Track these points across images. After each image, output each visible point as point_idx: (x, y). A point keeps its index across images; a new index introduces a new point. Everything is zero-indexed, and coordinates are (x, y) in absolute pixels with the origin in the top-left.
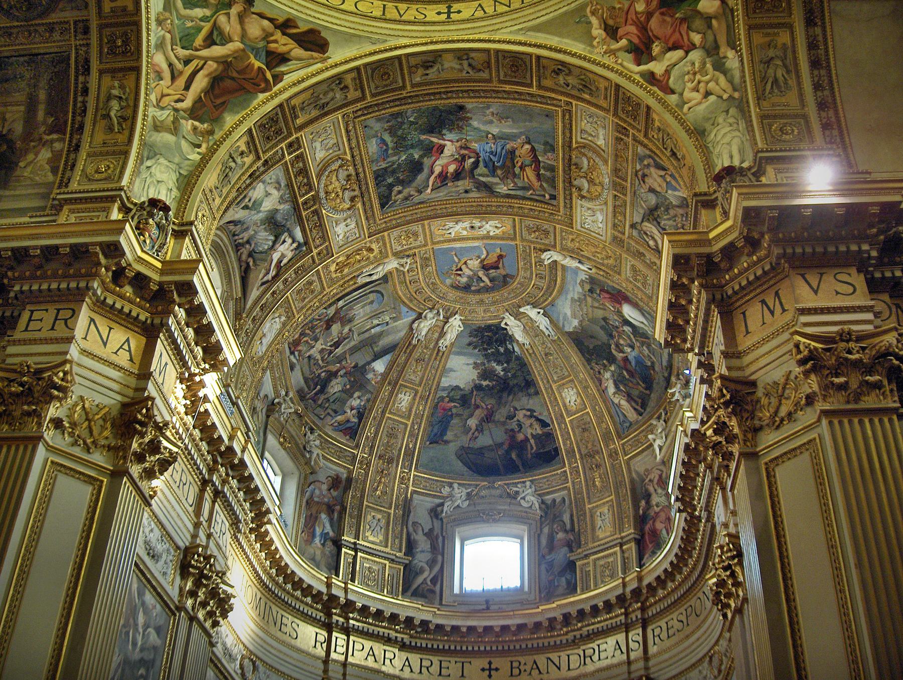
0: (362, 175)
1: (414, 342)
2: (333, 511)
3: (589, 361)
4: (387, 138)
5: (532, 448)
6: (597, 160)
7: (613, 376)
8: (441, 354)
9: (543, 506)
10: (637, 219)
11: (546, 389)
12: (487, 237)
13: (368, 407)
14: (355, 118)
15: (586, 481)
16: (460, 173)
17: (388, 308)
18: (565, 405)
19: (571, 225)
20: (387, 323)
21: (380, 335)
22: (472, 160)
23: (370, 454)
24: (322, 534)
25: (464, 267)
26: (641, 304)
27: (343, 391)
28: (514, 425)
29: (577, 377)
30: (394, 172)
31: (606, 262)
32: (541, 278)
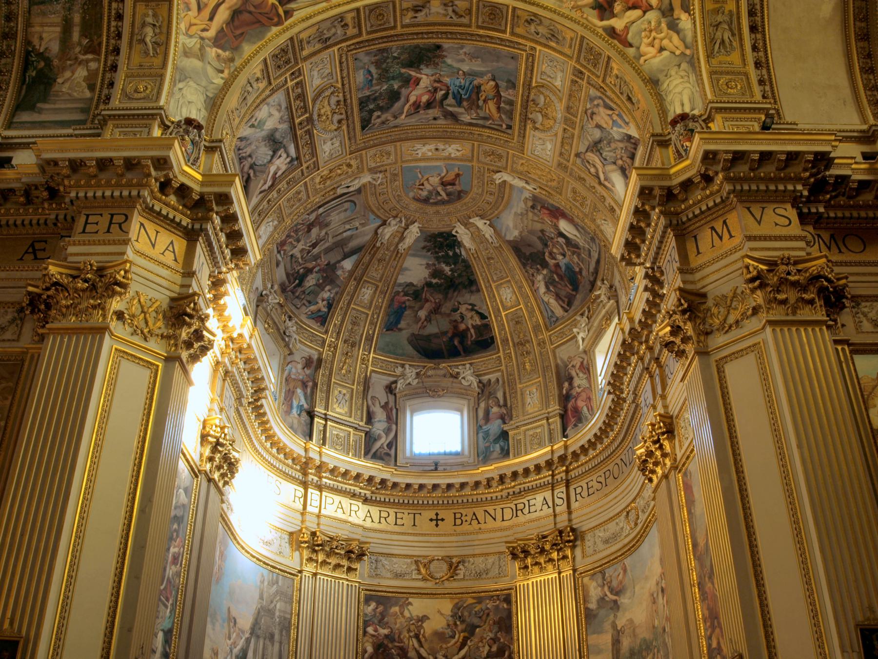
0: (349, 101)
1: (378, 244)
2: (306, 387)
3: (524, 265)
4: (373, 70)
5: (472, 336)
6: (553, 98)
7: (544, 278)
9: (481, 385)
10: (582, 149)
11: (486, 287)
12: (449, 158)
13: (337, 298)
14: (349, 51)
15: (518, 365)
16: (432, 103)
18: (501, 302)
20: (357, 228)
21: (351, 238)
22: (443, 92)
23: (337, 339)
24: (298, 406)
25: (426, 183)
26: (576, 219)
27: (316, 285)
28: (456, 316)
29: (513, 278)
30: (375, 99)
31: (549, 183)
32: (491, 194)
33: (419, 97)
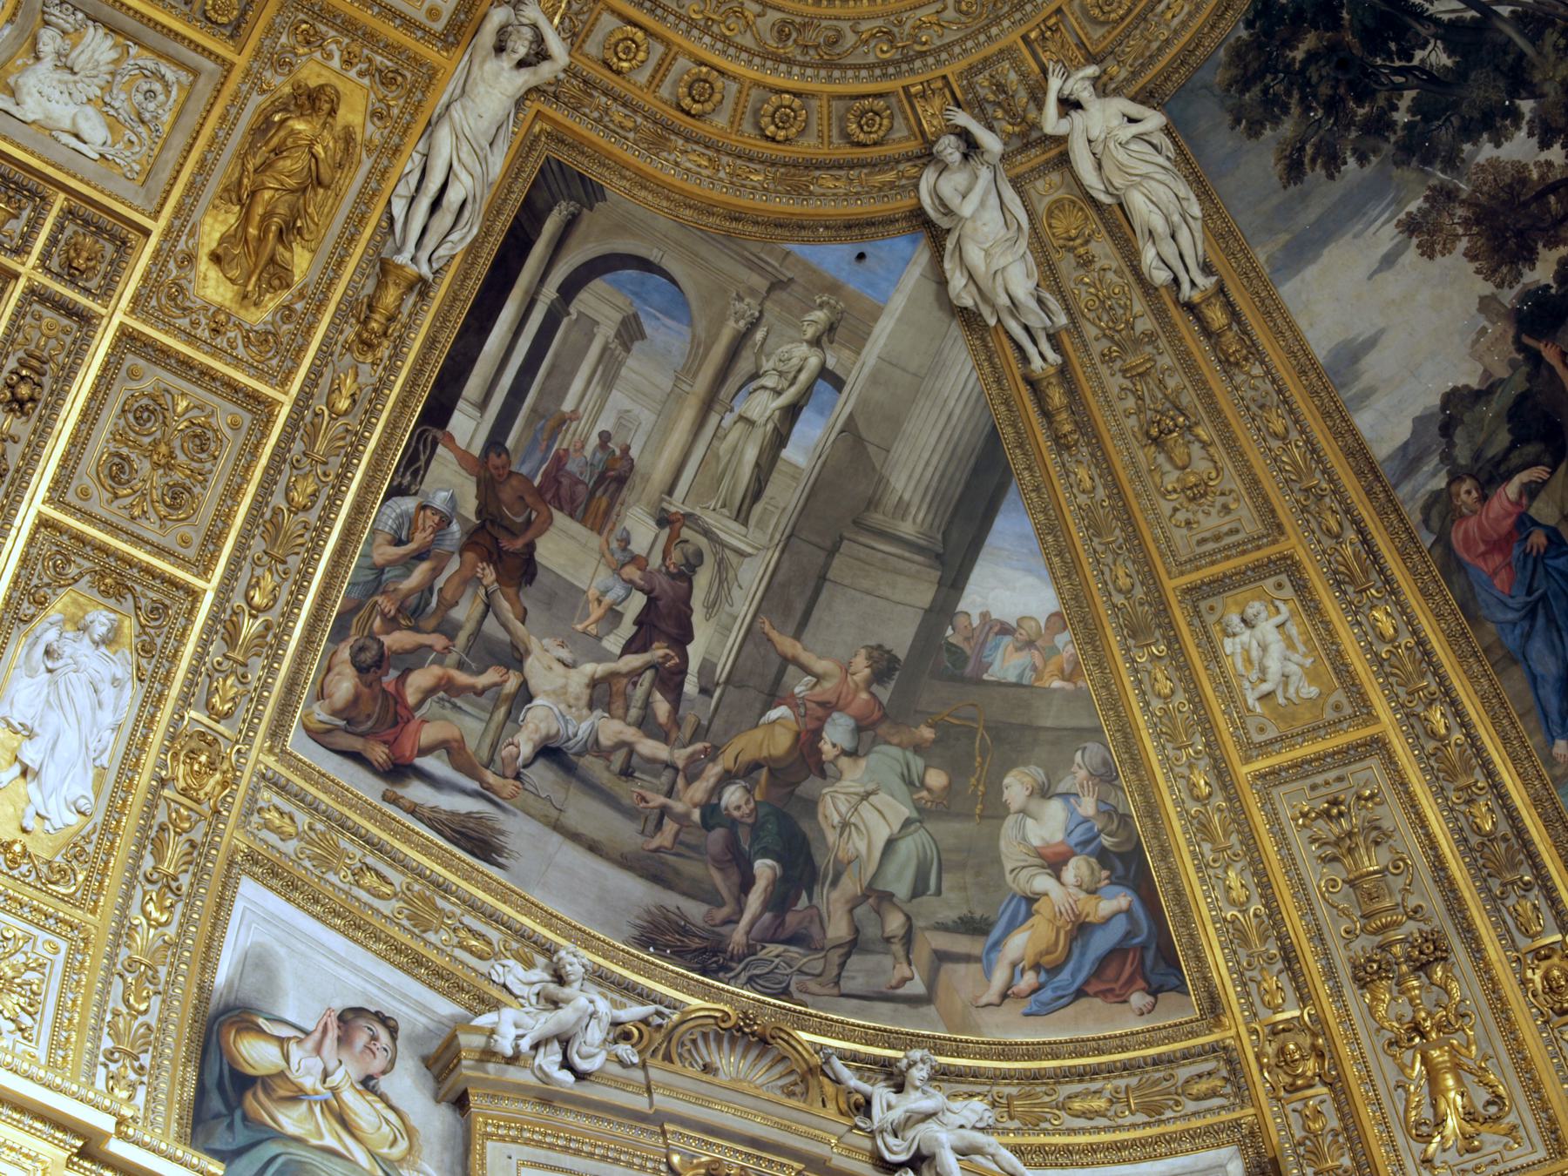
8: (1217, 316)
17: (749, 306)
20: (824, 373)
27: (924, 814)
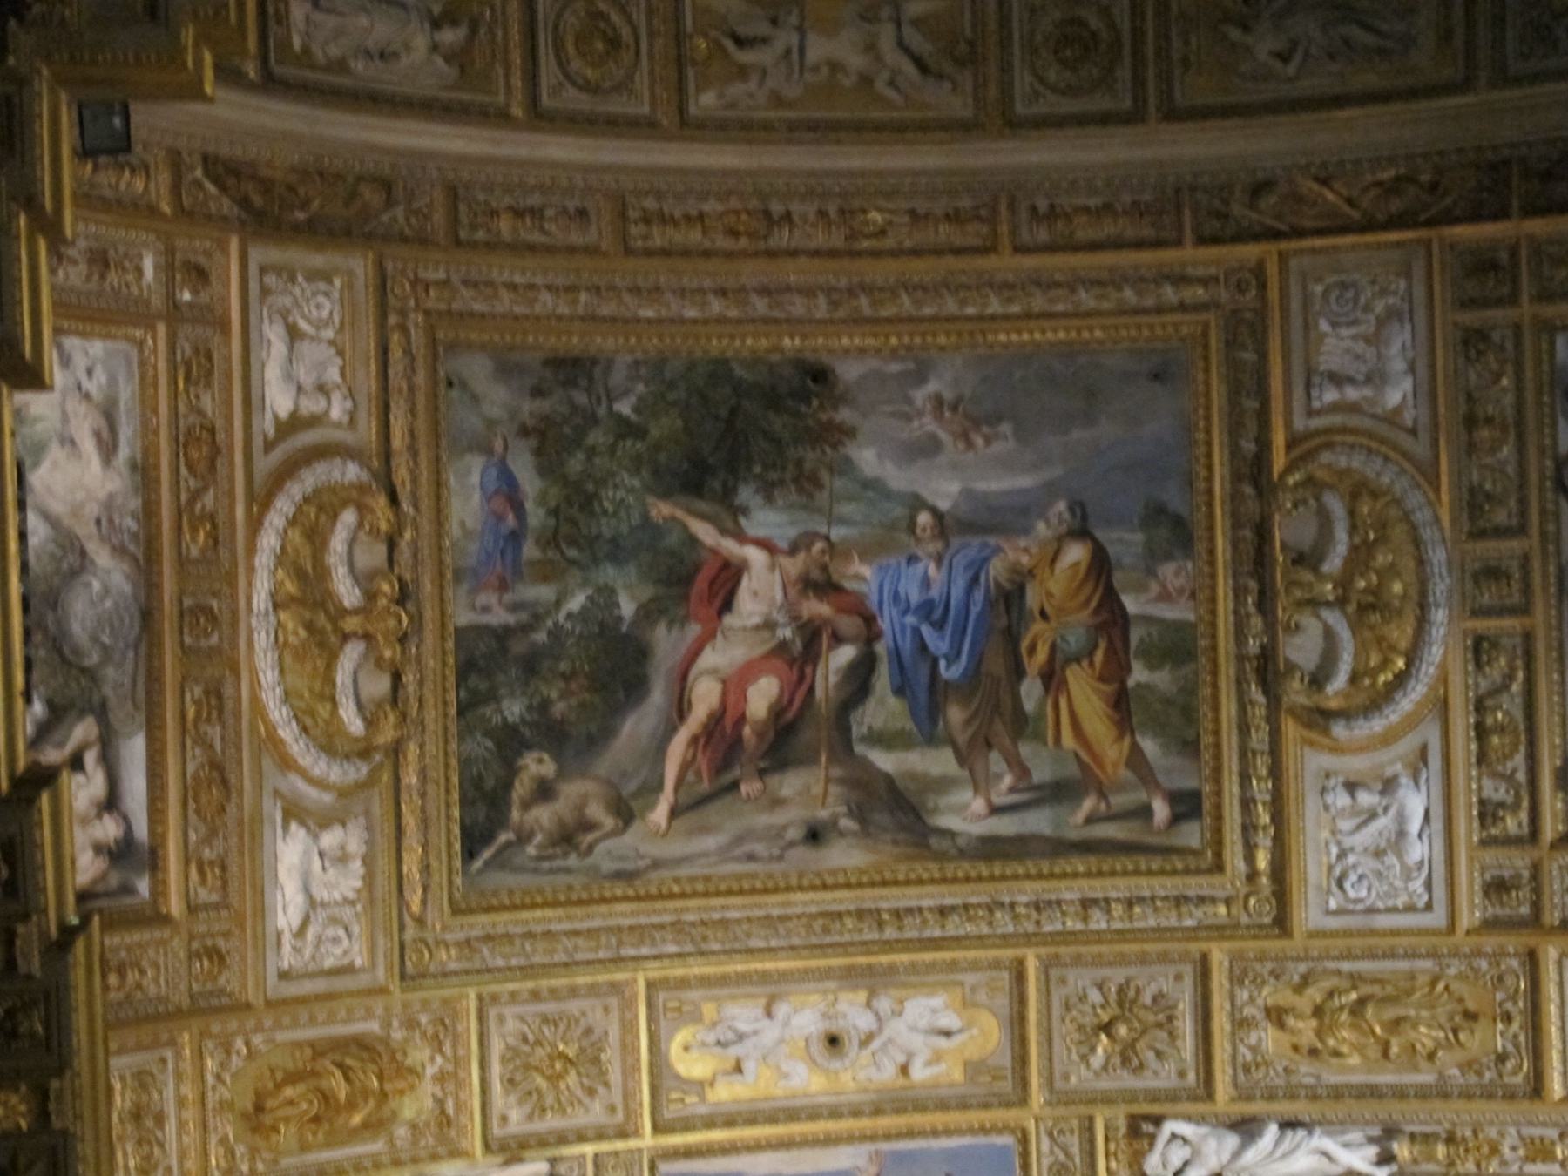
4: (529, 482)
19: (1282, 923)
22: (845, 655)
30: (531, 666)
33: (735, 684)
